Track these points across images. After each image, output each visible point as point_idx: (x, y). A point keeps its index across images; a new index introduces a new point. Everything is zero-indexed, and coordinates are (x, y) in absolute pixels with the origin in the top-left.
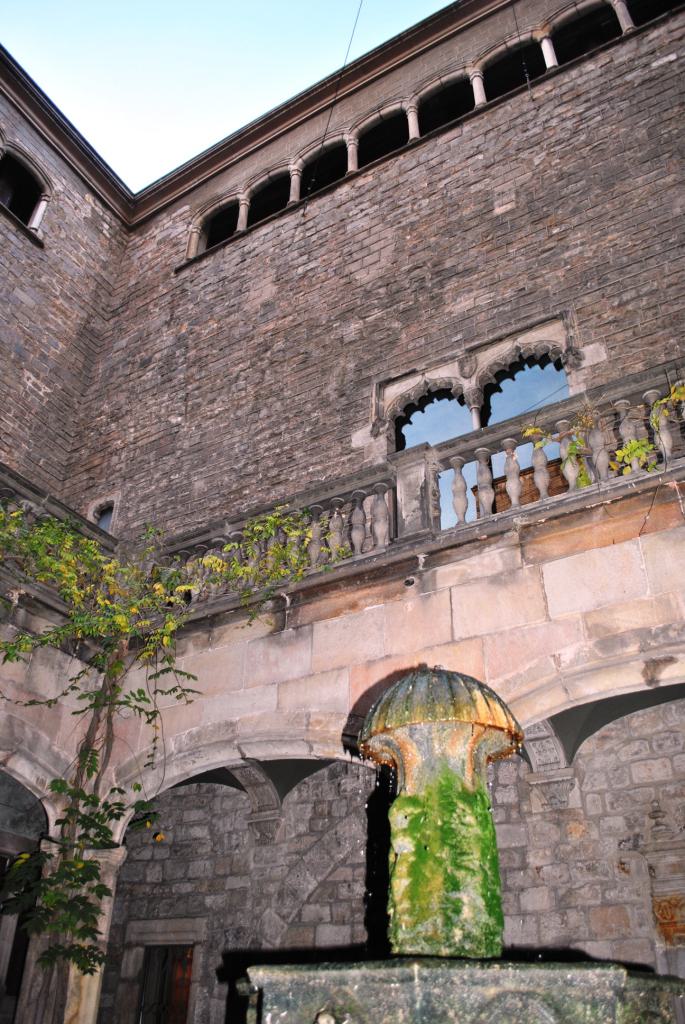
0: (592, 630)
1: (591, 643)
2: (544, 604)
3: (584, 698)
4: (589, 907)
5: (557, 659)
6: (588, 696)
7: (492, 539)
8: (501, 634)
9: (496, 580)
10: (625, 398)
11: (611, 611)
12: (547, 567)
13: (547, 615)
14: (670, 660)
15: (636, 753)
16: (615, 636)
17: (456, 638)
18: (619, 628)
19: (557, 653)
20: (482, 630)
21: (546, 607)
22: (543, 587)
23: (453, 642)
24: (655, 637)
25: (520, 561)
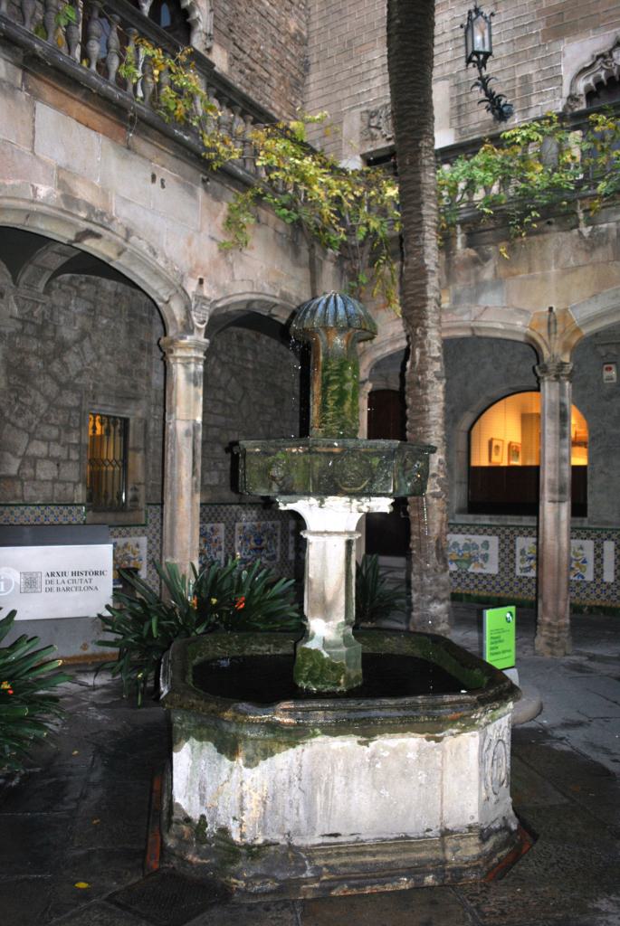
2: (32, 136)
3: (33, 228)
5: (35, 190)
6: (38, 229)
7: (53, 71)
10: (121, 17)
11: (75, 178)
13: (33, 148)
14: (98, 236)
16: (74, 199)
18: (77, 194)
19: (36, 185)
21: (33, 141)
22: (34, 120)
24: (96, 215)
25: (20, 81)
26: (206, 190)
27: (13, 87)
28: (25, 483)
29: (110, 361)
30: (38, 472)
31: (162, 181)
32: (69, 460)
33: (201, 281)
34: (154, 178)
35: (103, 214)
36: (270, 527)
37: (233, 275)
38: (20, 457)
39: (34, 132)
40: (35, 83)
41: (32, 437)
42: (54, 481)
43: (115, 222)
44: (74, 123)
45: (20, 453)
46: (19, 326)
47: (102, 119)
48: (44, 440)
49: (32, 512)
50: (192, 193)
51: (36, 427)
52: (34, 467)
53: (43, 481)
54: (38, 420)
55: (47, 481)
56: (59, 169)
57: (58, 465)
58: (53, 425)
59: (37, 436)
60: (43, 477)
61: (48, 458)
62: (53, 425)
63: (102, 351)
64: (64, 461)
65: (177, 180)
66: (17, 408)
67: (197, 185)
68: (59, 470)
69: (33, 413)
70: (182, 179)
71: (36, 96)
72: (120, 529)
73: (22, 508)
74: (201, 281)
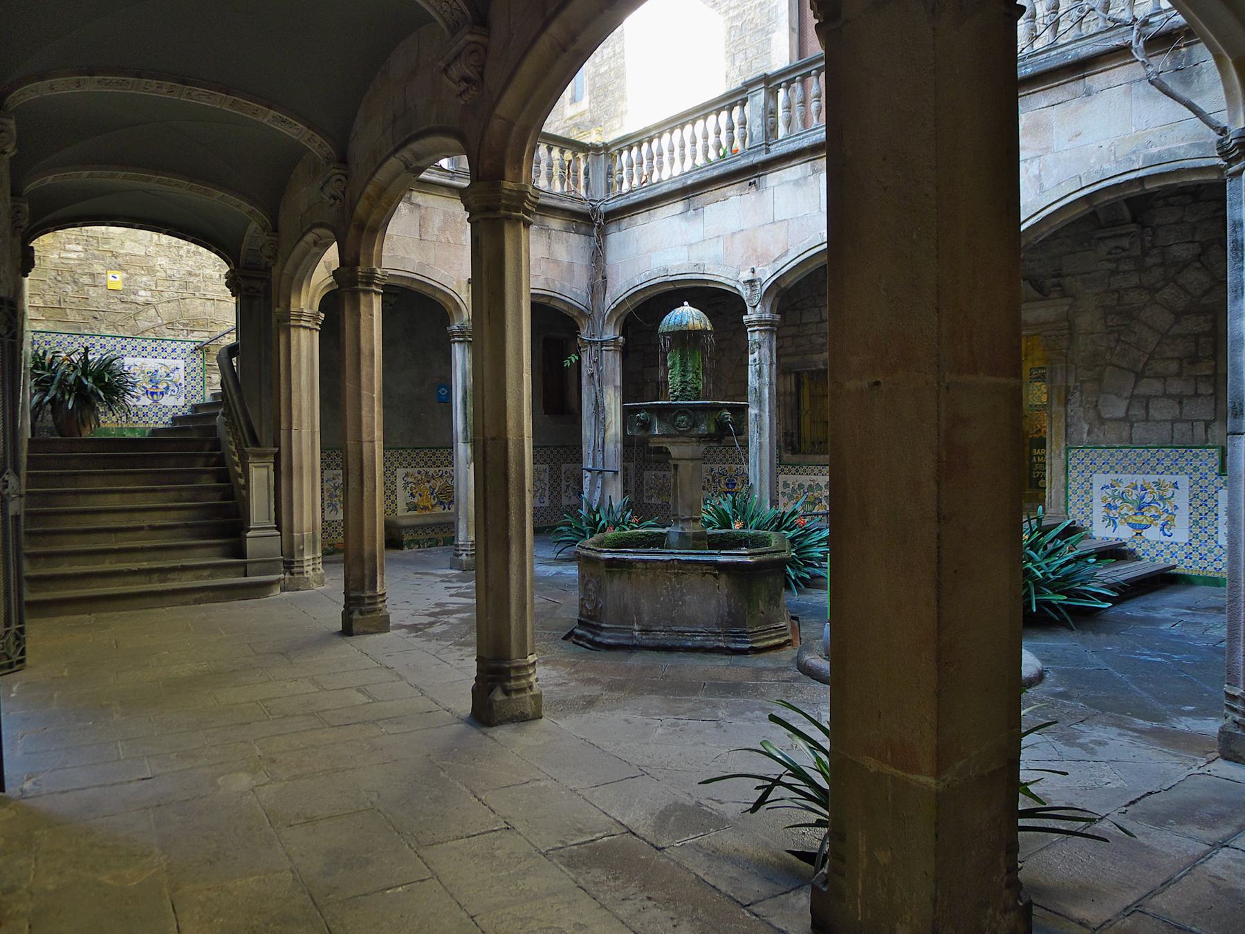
9: (797, 183)
17: (776, 218)
27: (805, 178)
28: (1135, 425)
30: (1151, 411)
32: (1197, 395)
37: (1041, 186)
38: (1127, 398)
41: (1139, 376)
42: (1173, 422)
45: (1126, 395)
46: (1112, 266)
48: (1157, 376)
49: (1139, 455)
51: (1146, 364)
52: (1147, 408)
53: (1158, 422)
54: (1147, 356)
55: (1167, 421)
57: (1180, 403)
58: (1168, 359)
59: (1147, 373)
60: (1158, 417)
61: (1166, 395)
62: (1168, 359)
64: (1189, 397)
66: (1118, 348)
68: (1181, 409)
69: (1139, 350)
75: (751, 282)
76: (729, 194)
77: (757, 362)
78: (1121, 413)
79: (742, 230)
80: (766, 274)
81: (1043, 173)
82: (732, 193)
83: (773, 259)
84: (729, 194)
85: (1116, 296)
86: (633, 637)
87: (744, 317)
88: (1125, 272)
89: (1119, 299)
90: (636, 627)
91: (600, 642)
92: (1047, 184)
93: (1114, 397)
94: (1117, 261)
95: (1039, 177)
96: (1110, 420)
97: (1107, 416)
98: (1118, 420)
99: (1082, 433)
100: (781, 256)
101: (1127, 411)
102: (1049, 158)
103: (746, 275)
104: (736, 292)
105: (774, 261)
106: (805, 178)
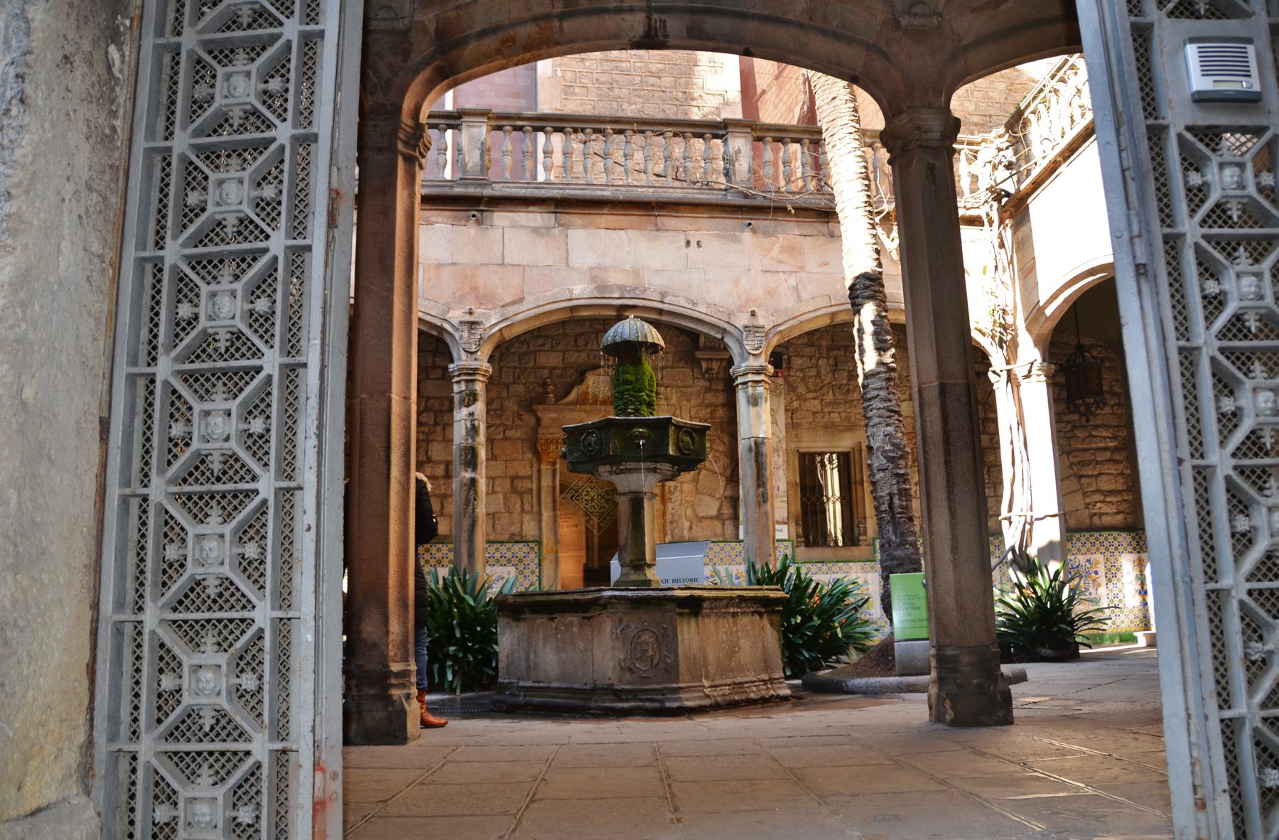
0: (594, 279)
1: (592, 287)
4: (494, 439)
8: (537, 267)
9: (535, 230)
12: (570, 231)
15: (541, 346)
17: (507, 261)
20: (524, 262)
21: (567, 258)
23: (503, 264)
26: (754, 231)
29: (815, 399)
31: (698, 243)
33: (753, 314)
34: (688, 243)
35: (635, 289)
36: (1083, 563)
37: (799, 296)
39: (567, 252)
40: (565, 218)
43: (648, 291)
44: (603, 231)
47: (629, 218)
49: (733, 548)
50: (736, 240)
56: (591, 269)
63: (802, 390)
65: (717, 236)
67: (742, 231)
70: (721, 233)
71: (566, 226)
72: (840, 564)
73: (722, 545)
74: (753, 314)
75: (472, 325)
76: (434, 219)
77: (476, 417)
78: (713, 512)
79: (454, 264)
80: (492, 320)
81: (800, 286)
82: (440, 220)
83: (501, 304)
84: (434, 219)
85: (709, 410)
86: (707, 696)
87: (451, 366)
88: (717, 391)
89: (711, 413)
90: (706, 683)
91: (679, 708)
92: (805, 296)
93: (708, 498)
94: (710, 380)
95: (796, 288)
96: (704, 518)
97: (702, 514)
98: (711, 518)
99: (682, 529)
100: (513, 303)
101: (719, 510)
102: (803, 275)
103: (456, 315)
104: (435, 333)
105: (504, 306)
106: (548, 228)
